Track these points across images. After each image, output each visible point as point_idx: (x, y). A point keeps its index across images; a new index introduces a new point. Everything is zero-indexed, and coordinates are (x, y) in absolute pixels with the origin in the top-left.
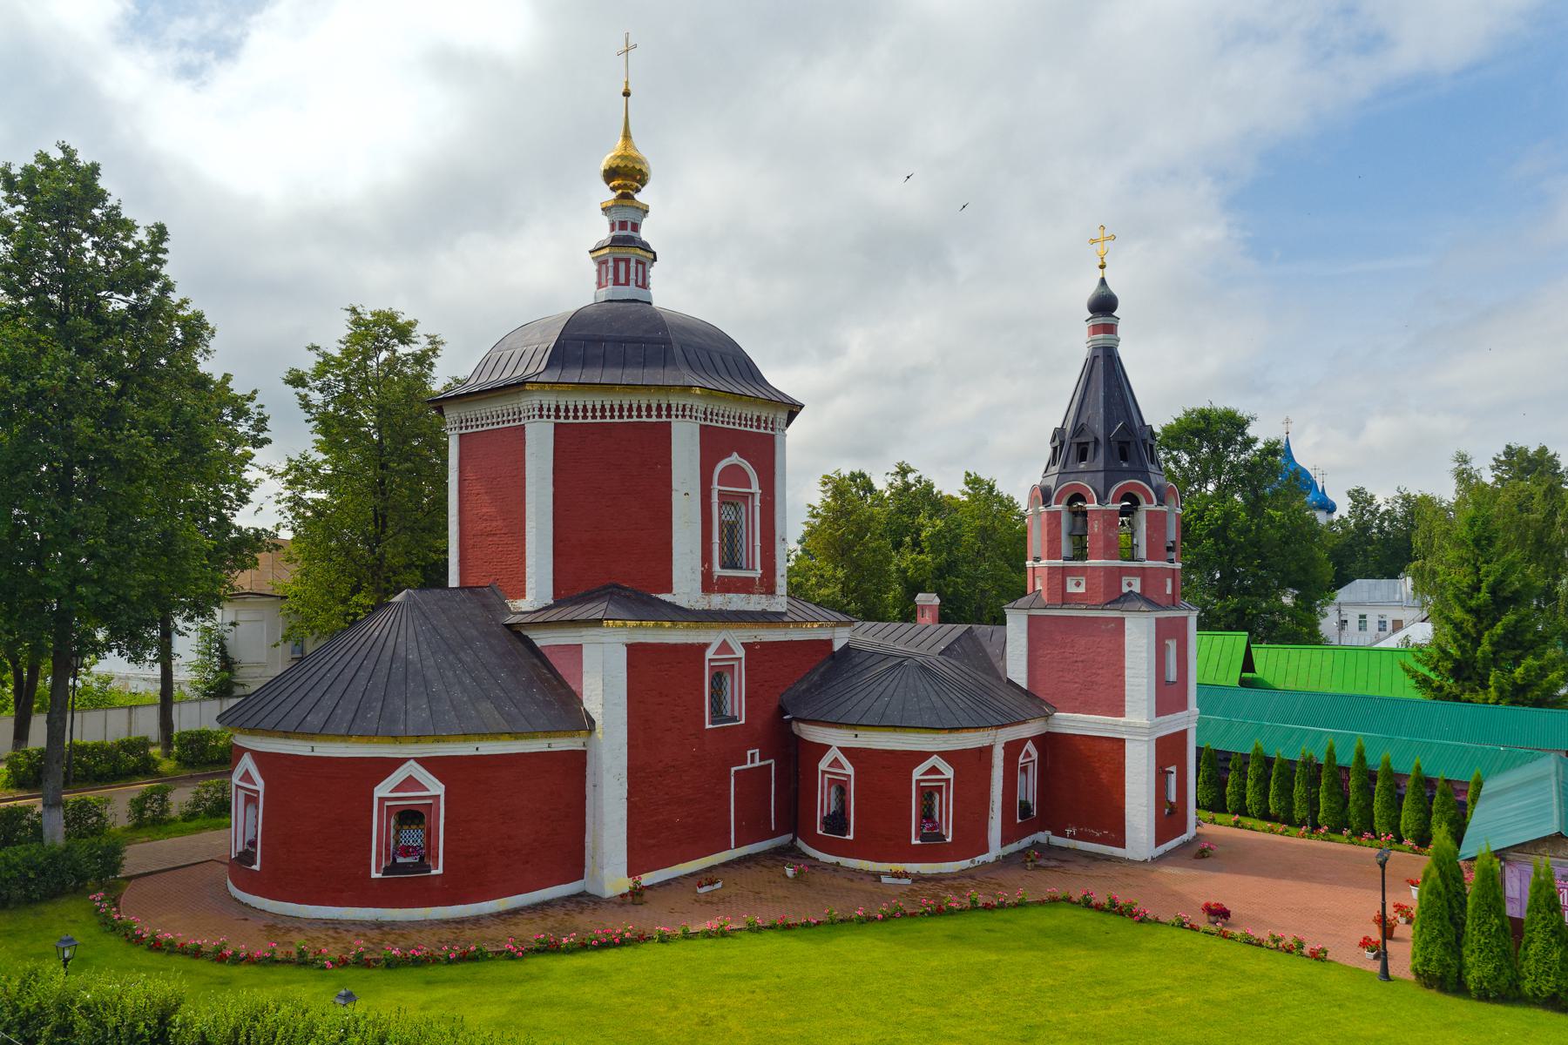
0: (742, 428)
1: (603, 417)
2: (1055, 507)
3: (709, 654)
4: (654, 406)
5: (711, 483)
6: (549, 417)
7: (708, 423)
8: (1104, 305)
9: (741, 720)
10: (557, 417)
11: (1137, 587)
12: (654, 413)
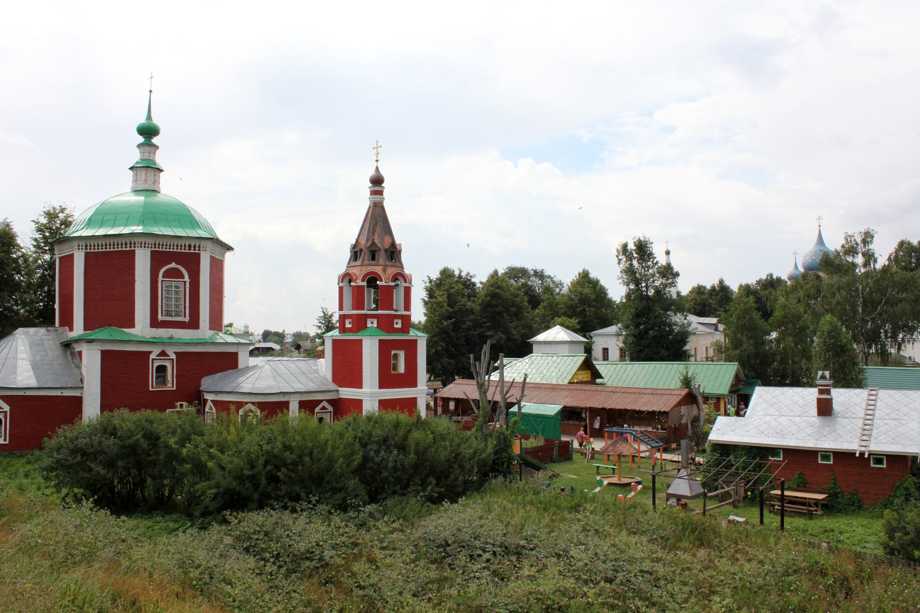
0: (179, 250)
1: (106, 248)
2: (341, 284)
3: (152, 356)
4: (128, 243)
5: (158, 277)
6: (82, 249)
7: (157, 249)
8: (377, 181)
9: (173, 387)
10: (86, 249)
11: (399, 326)
12: (128, 246)
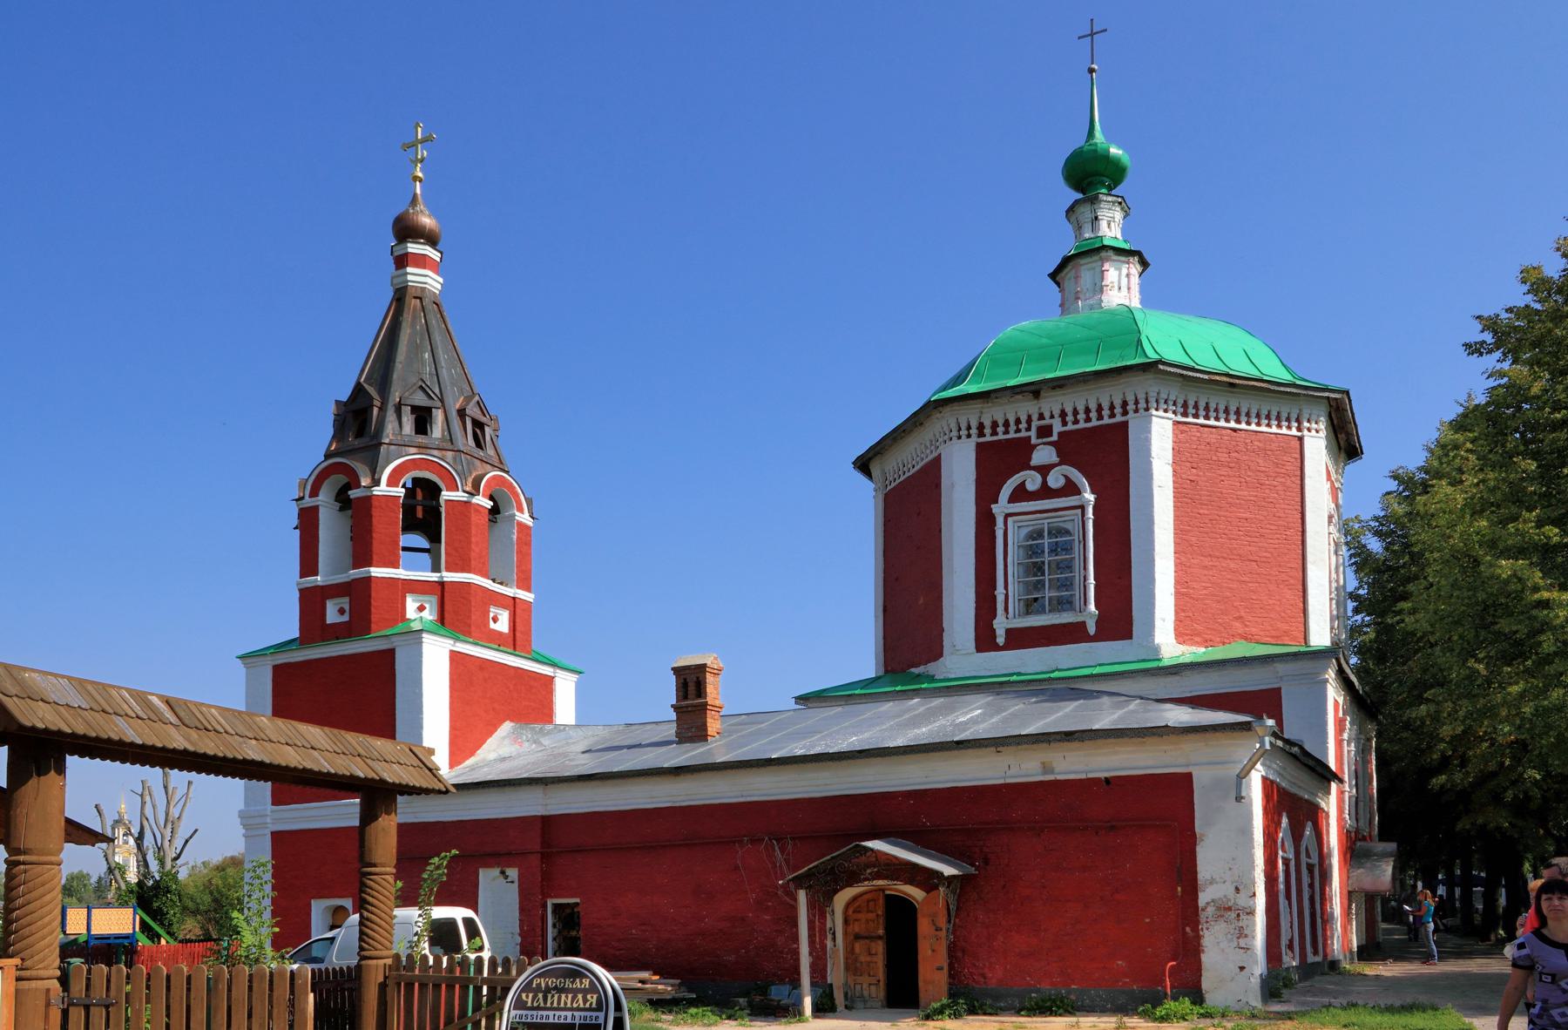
10: (981, 434)
